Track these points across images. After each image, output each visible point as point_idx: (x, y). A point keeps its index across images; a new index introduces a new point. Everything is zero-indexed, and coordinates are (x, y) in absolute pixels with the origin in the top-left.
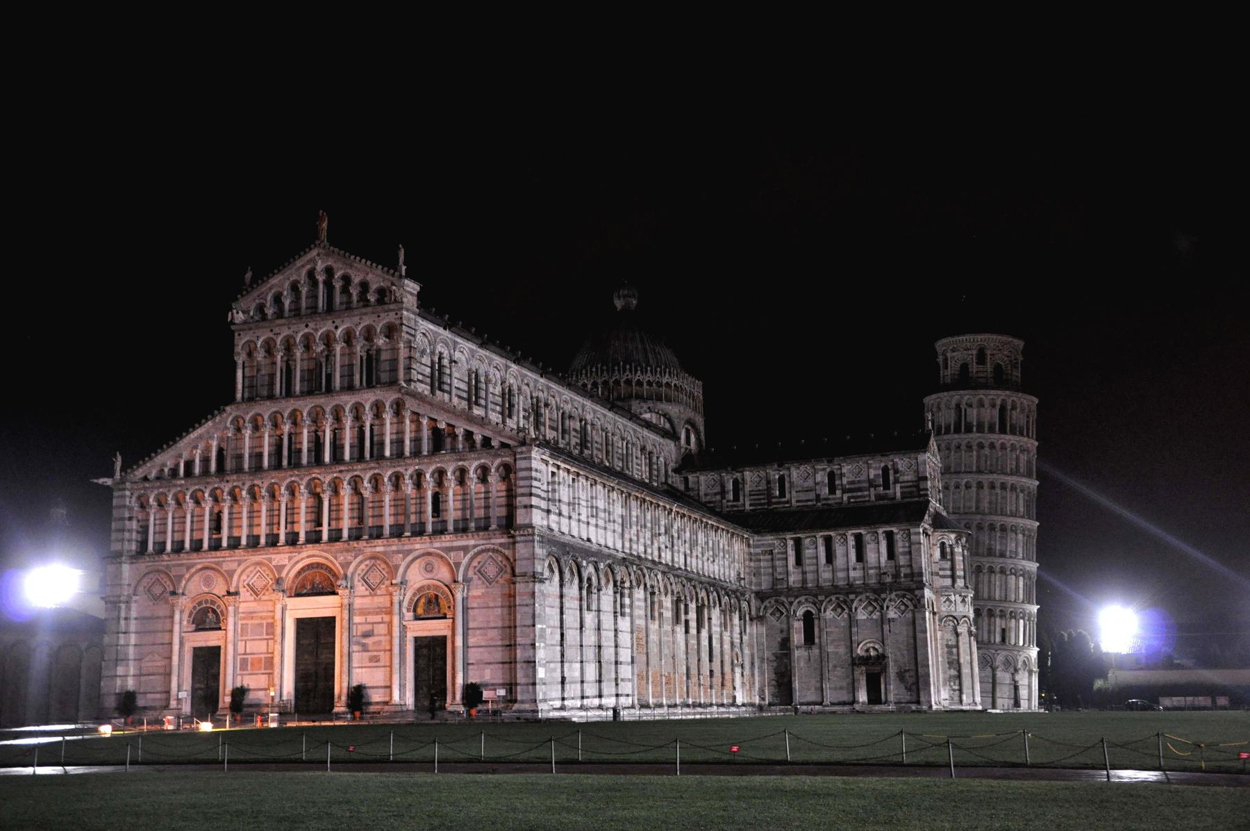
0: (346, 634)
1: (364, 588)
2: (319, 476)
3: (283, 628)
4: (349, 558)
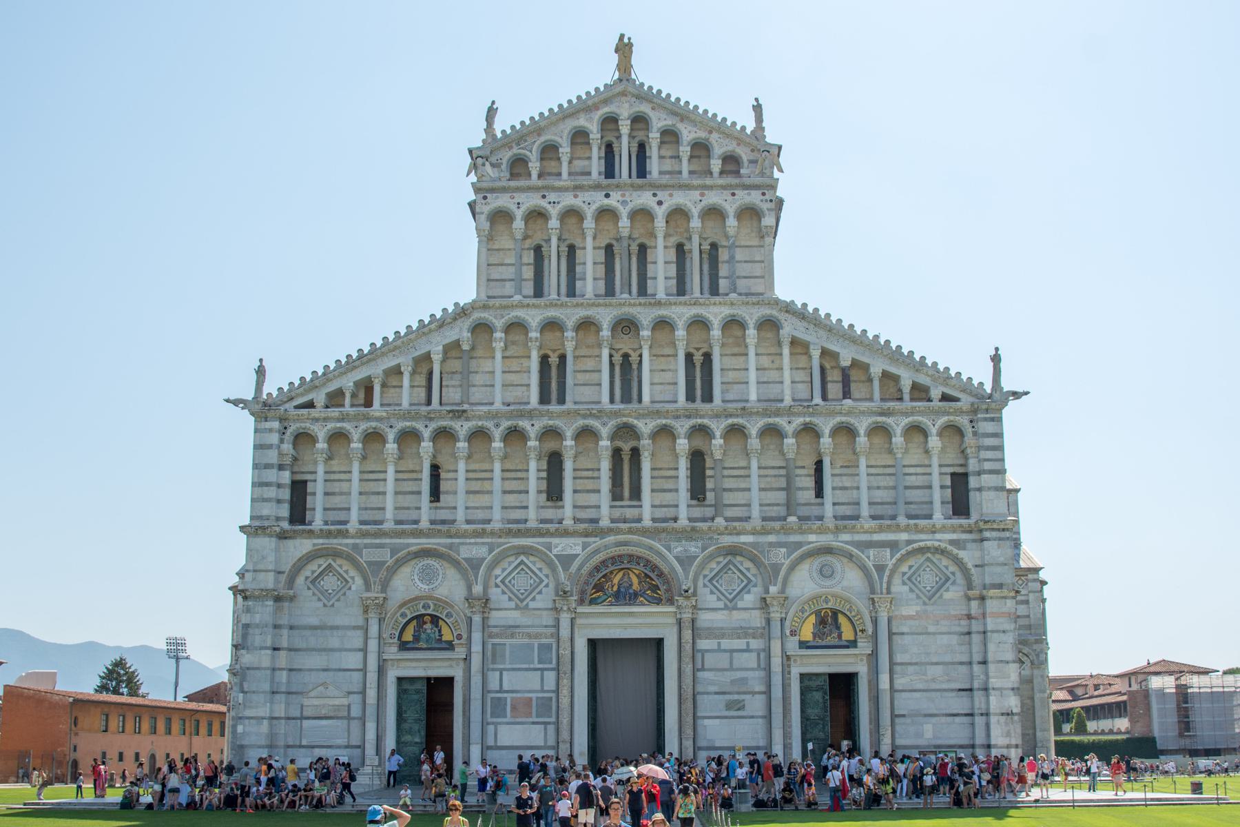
0: (690, 666)
1: (714, 597)
2: (635, 422)
3: (572, 653)
4: (693, 549)
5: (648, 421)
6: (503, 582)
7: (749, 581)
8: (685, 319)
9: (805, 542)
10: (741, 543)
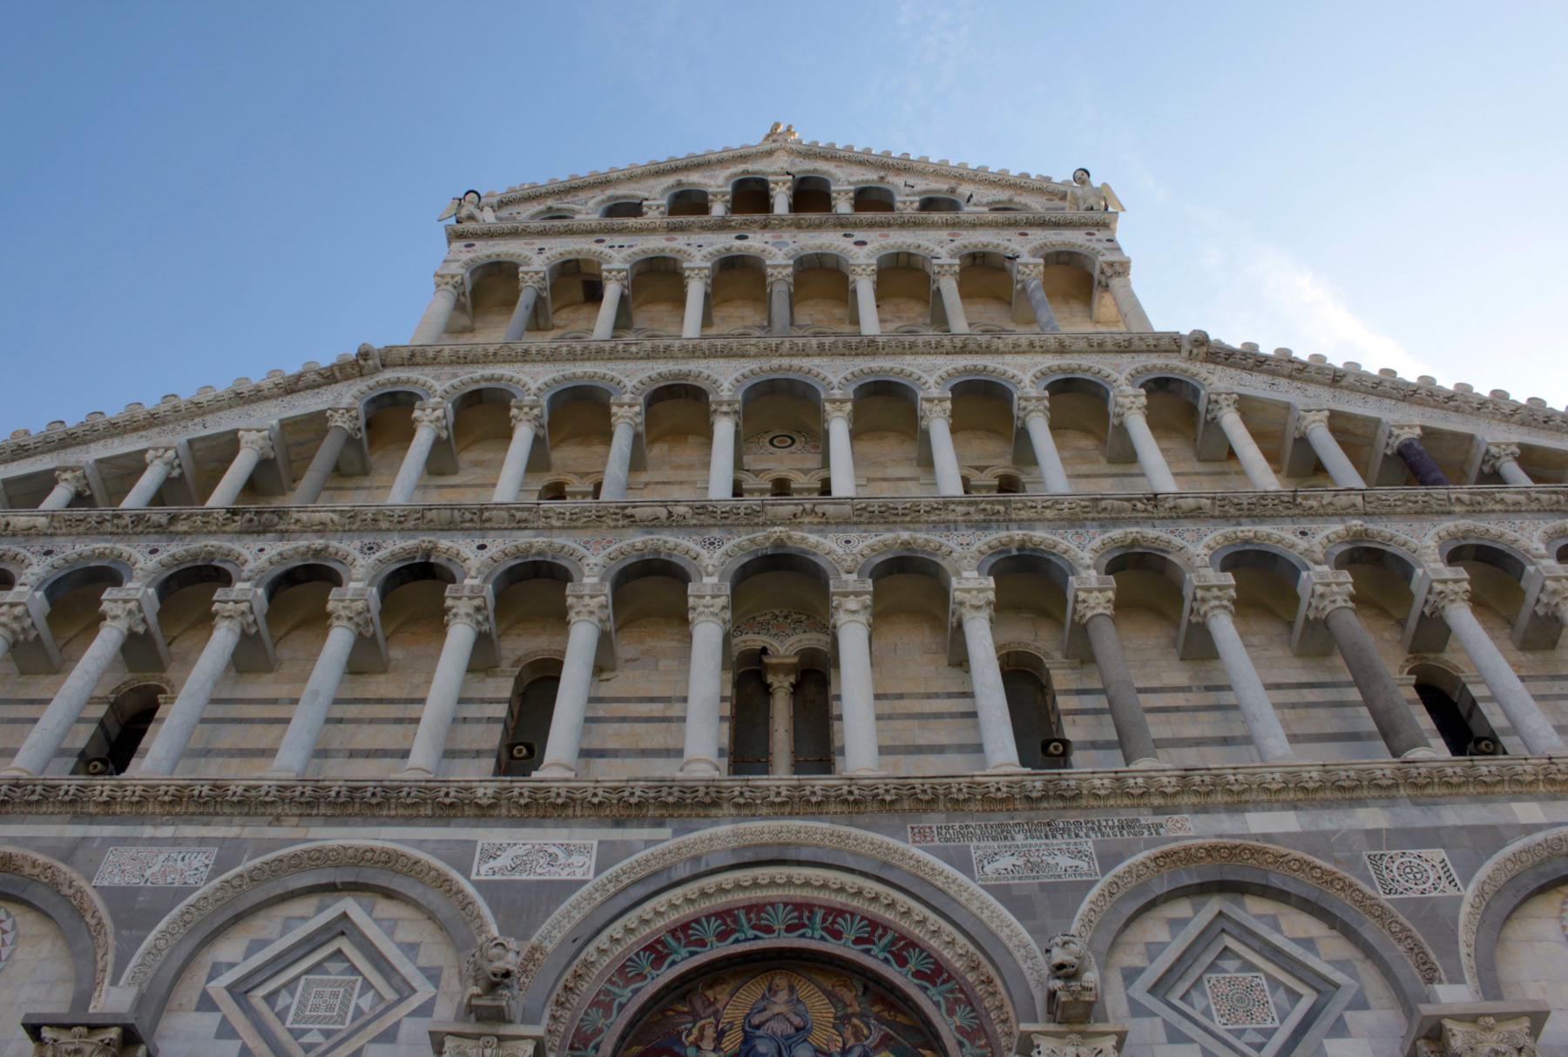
4: (1064, 861)
5: (853, 536)
6: (241, 991)
7: (1325, 988)
8: (942, 372)
9: (1510, 826)
10: (1256, 837)
